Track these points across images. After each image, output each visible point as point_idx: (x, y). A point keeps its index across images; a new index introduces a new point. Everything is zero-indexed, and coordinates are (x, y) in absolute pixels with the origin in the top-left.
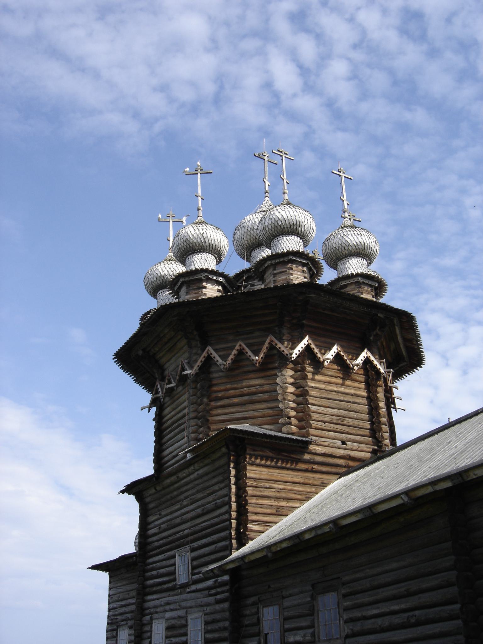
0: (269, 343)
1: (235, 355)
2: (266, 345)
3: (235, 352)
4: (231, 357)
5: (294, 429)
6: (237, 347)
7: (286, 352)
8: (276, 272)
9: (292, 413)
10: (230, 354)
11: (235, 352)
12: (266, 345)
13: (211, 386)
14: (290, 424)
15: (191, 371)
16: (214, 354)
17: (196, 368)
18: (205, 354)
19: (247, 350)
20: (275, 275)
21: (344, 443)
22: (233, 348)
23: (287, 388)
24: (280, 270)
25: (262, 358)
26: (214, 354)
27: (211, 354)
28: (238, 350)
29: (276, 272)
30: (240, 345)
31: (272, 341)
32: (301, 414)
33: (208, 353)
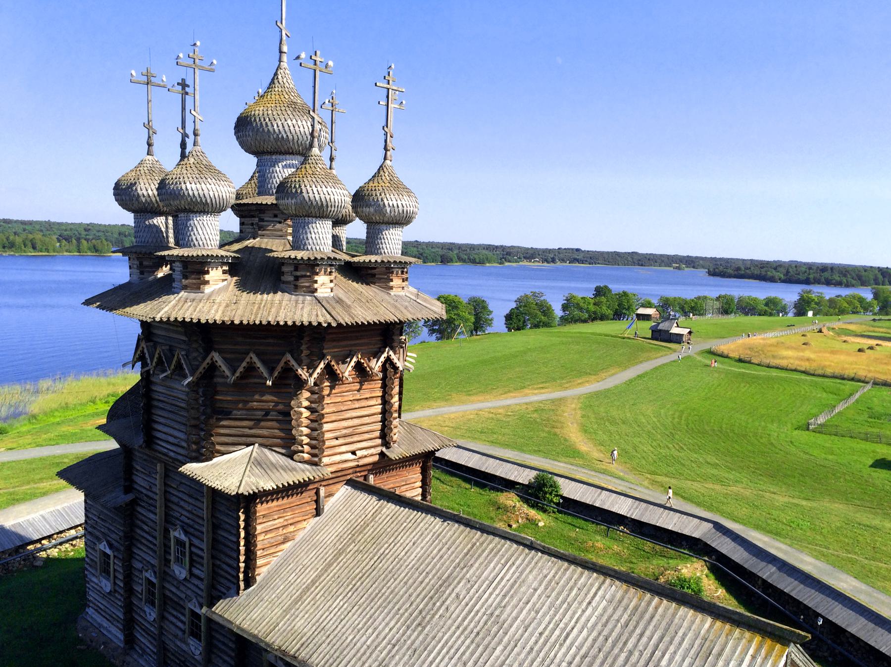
0: (285, 363)
1: (244, 367)
2: (282, 364)
3: (244, 364)
4: (241, 369)
5: (306, 456)
6: (248, 360)
7: (304, 377)
8: (298, 273)
9: (306, 440)
10: (239, 366)
11: (244, 364)
12: (282, 364)
13: (217, 393)
14: (303, 452)
15: (191, 378)
16: (220, 362)
17: (197, 374)
18: (208, 360)
19: (259, 364)
20: (297, 278)
21: (354, 453)
22: (242, 360)
23: (301, 414)
24: (303, 273)
25: (276, 377)
26: (220, 362)
27: (216, 361)
28: (248, 363)
29: (298, 273)
30: (251, 358)
31: (289, 361)
32: (314, 442)
33: (212, 359)
